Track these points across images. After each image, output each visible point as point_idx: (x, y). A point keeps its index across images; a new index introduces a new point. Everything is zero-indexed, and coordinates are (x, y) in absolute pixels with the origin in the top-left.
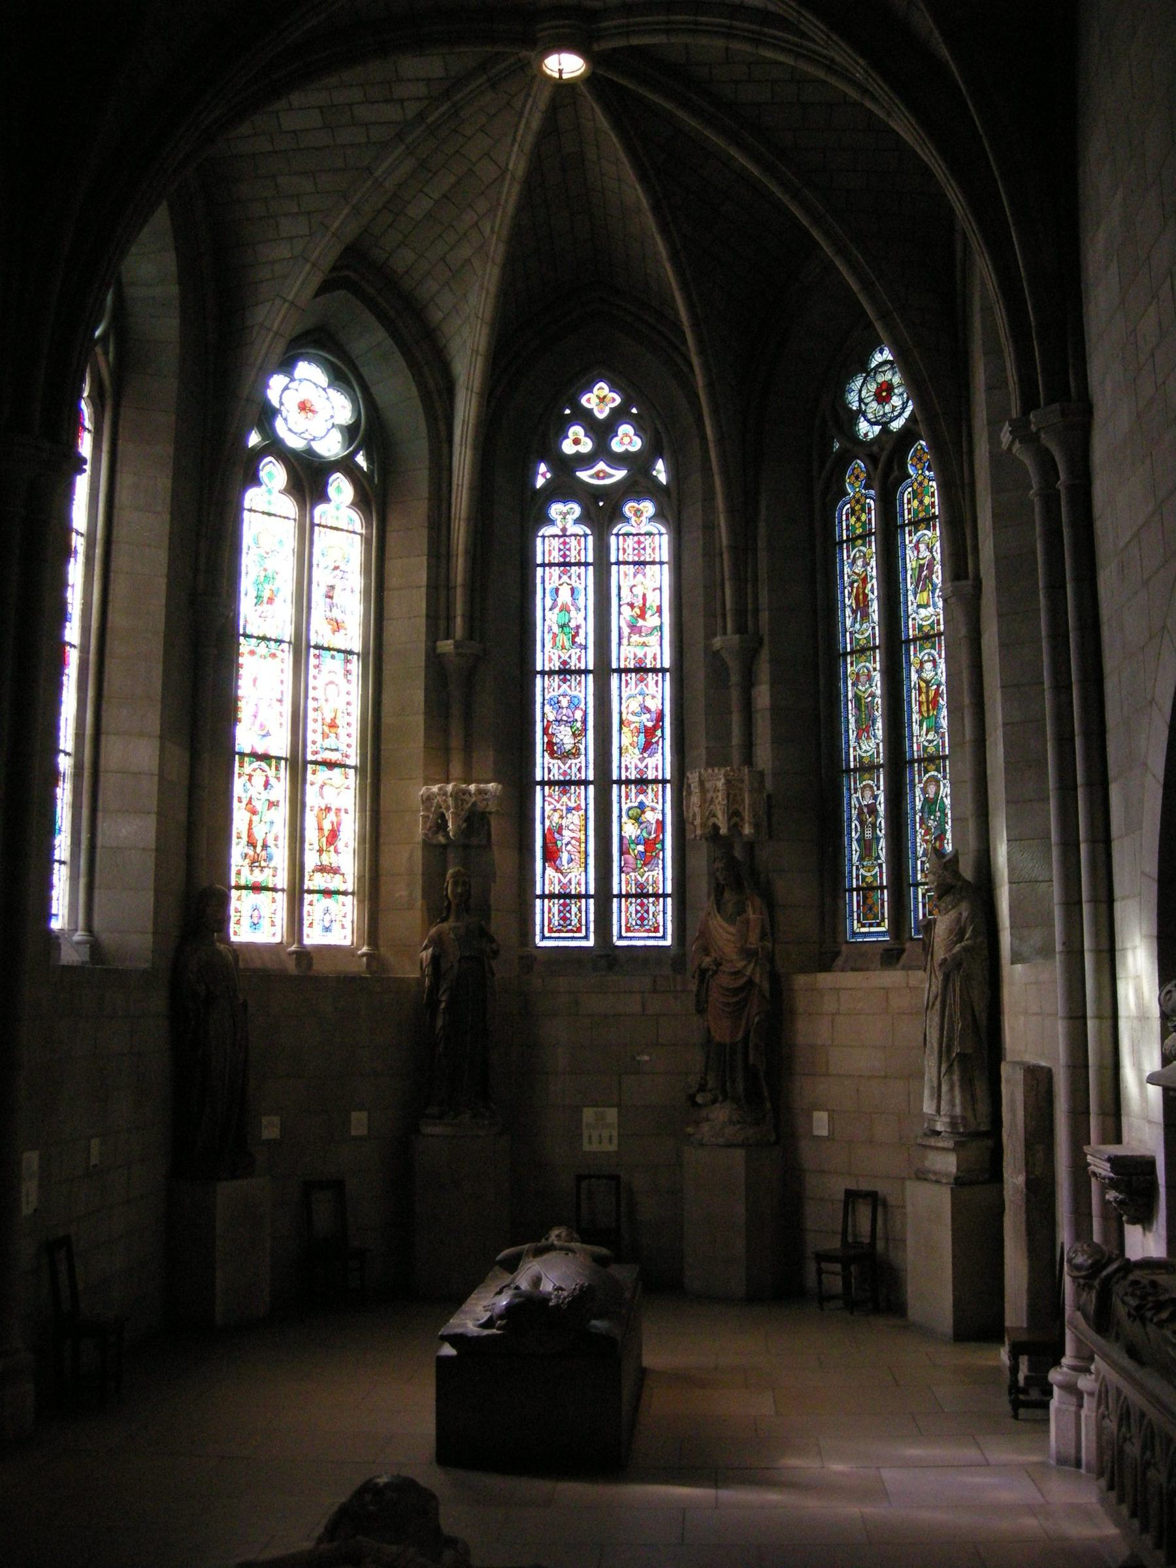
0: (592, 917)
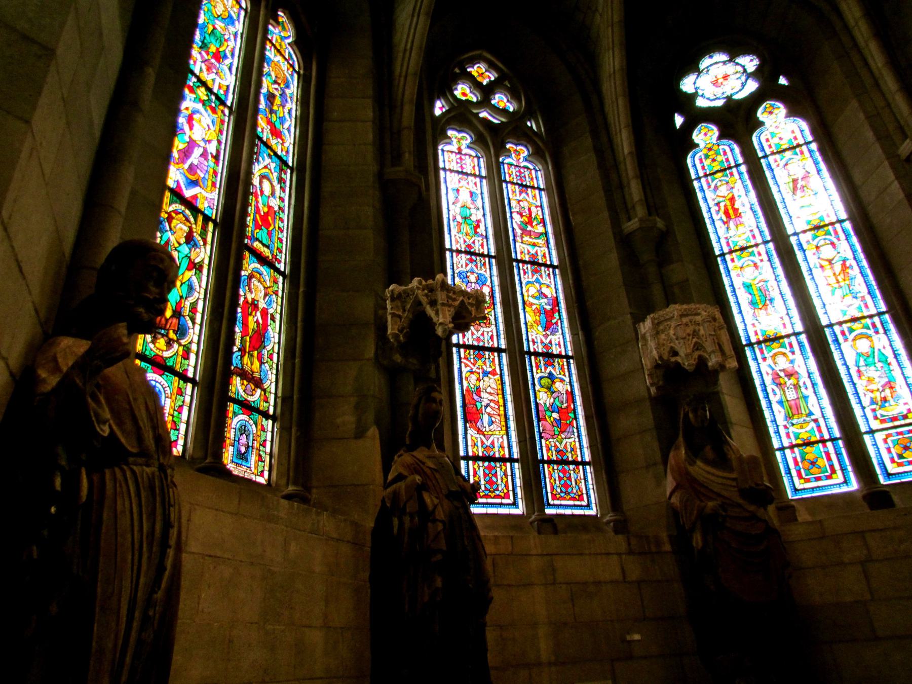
0: (518, 482)
